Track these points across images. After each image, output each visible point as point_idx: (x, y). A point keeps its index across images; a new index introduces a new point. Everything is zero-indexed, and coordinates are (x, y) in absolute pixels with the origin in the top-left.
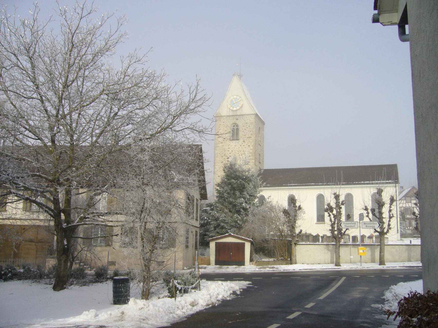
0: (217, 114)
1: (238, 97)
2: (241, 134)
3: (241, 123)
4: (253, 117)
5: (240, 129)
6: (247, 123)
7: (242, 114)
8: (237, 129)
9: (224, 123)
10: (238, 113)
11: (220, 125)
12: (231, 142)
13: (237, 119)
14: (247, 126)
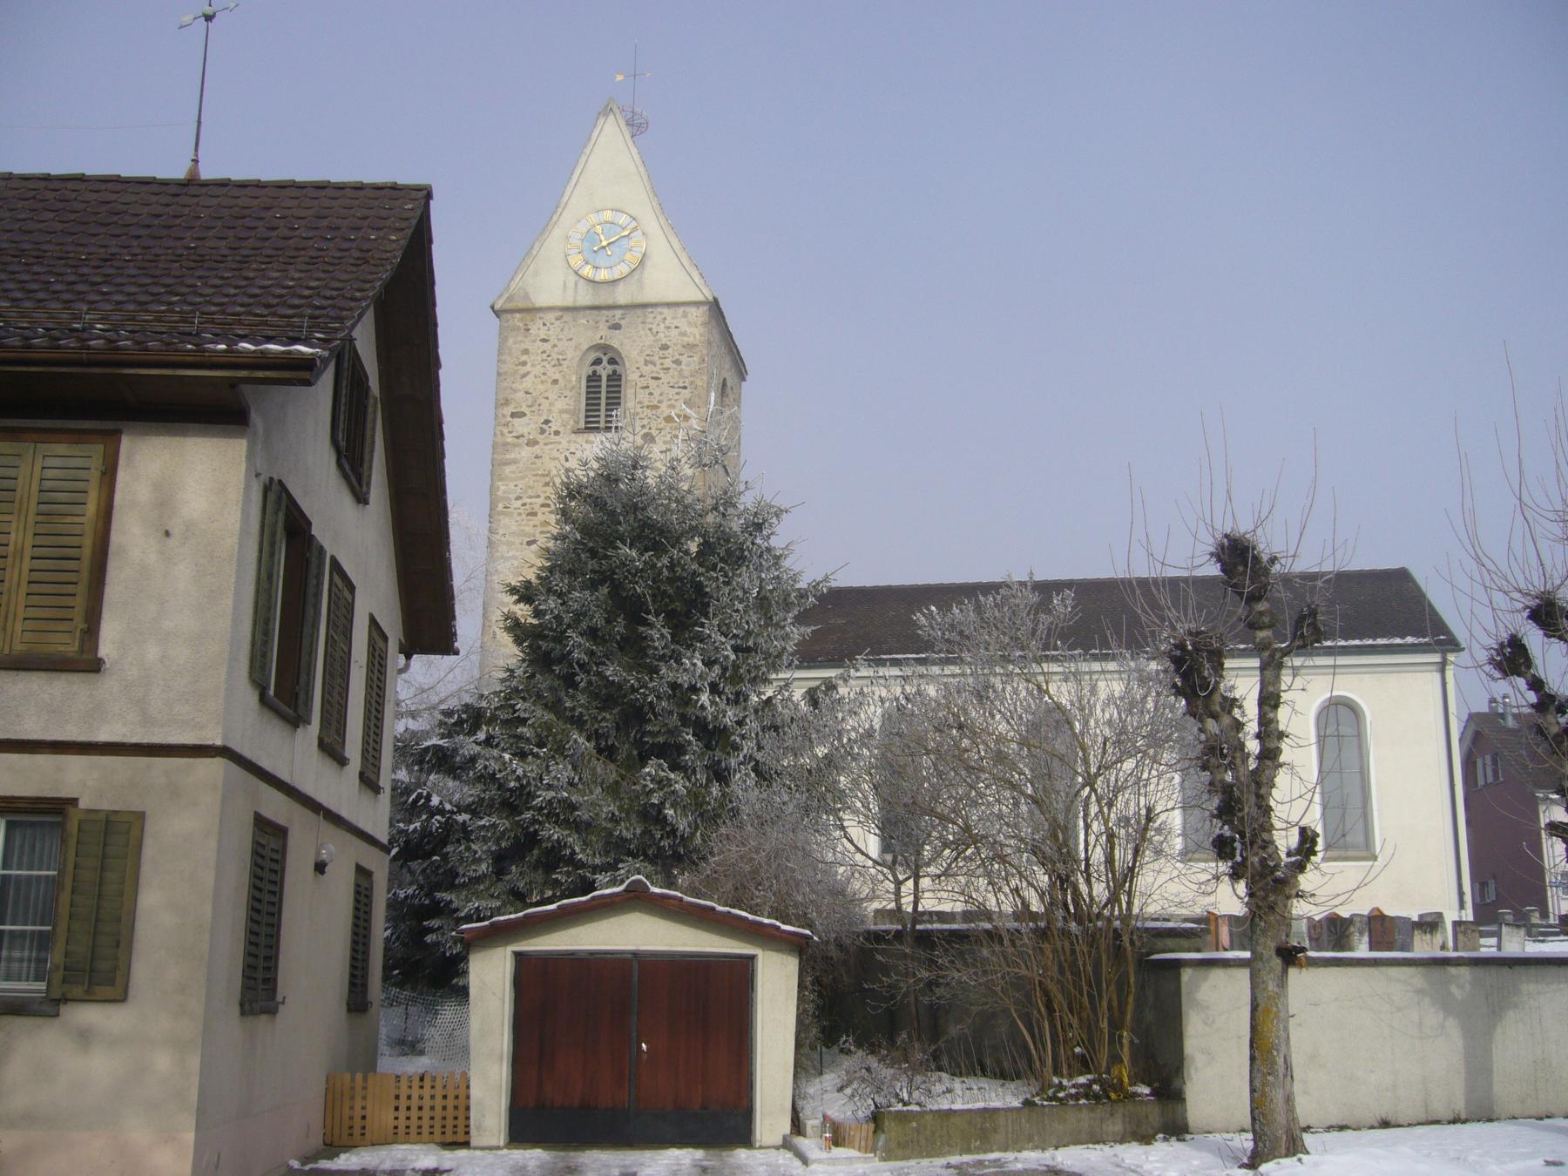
0: (510, 299)
1: (623, 219)
2: (632, 399)
3: (633, 346)
4: (698, 315)
5: (631, 375)
6: (665, 347)
7: (640, 299)
8: (615, 378)
9: (547, 346)
10: (622, 296)
11: (526, 352)
12: (581, 438)
13: (617, 327)
14: (668, 363)
